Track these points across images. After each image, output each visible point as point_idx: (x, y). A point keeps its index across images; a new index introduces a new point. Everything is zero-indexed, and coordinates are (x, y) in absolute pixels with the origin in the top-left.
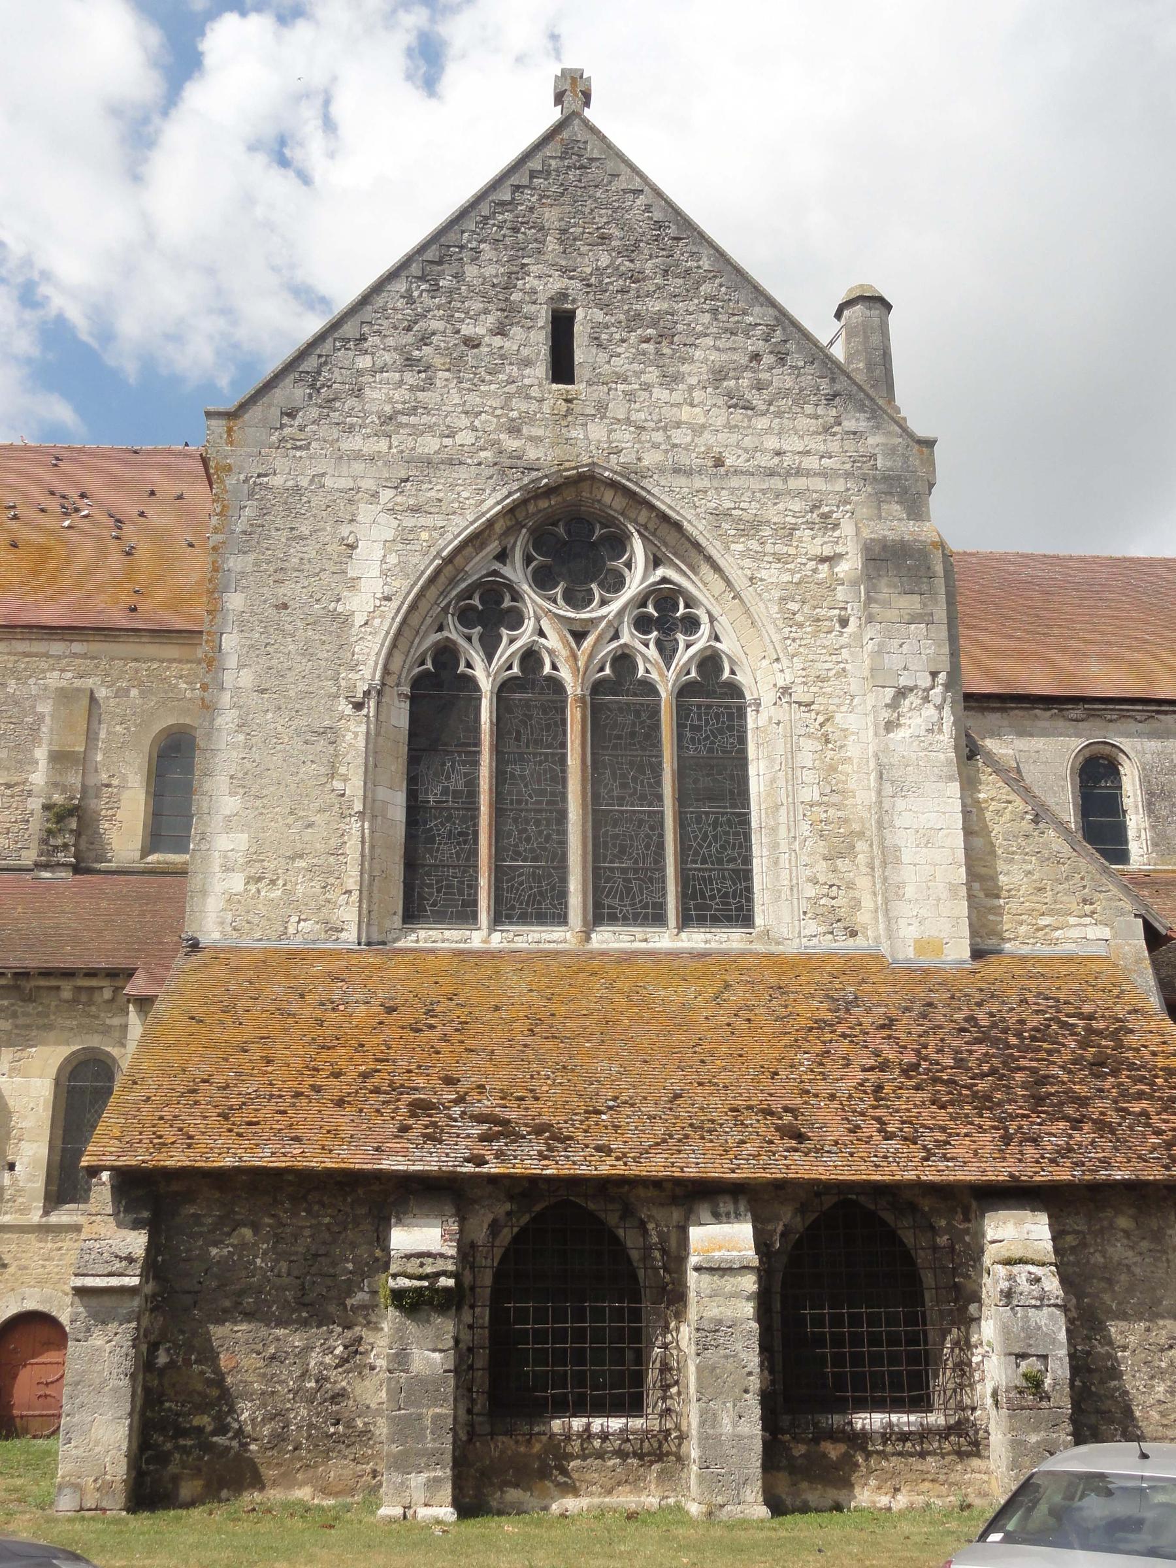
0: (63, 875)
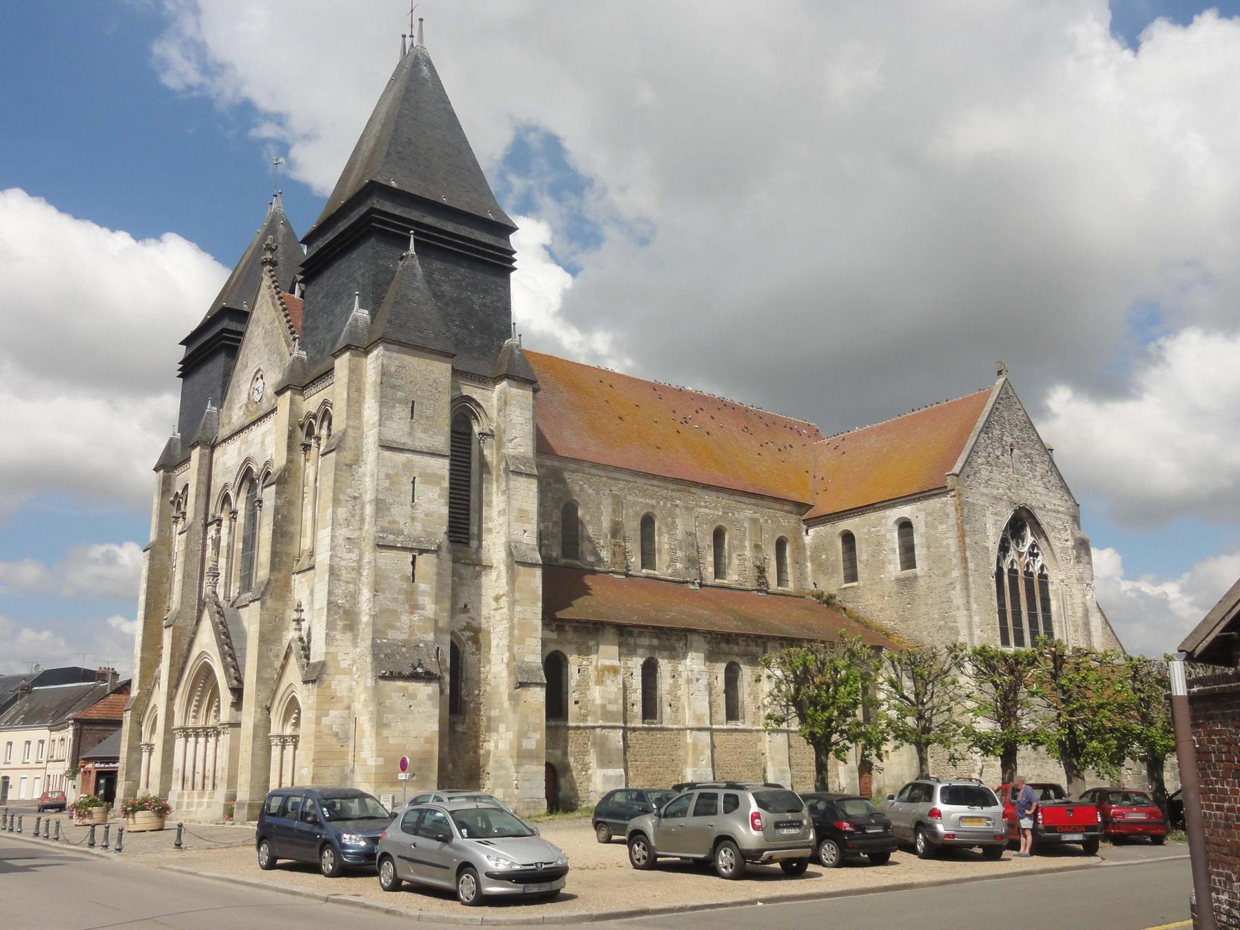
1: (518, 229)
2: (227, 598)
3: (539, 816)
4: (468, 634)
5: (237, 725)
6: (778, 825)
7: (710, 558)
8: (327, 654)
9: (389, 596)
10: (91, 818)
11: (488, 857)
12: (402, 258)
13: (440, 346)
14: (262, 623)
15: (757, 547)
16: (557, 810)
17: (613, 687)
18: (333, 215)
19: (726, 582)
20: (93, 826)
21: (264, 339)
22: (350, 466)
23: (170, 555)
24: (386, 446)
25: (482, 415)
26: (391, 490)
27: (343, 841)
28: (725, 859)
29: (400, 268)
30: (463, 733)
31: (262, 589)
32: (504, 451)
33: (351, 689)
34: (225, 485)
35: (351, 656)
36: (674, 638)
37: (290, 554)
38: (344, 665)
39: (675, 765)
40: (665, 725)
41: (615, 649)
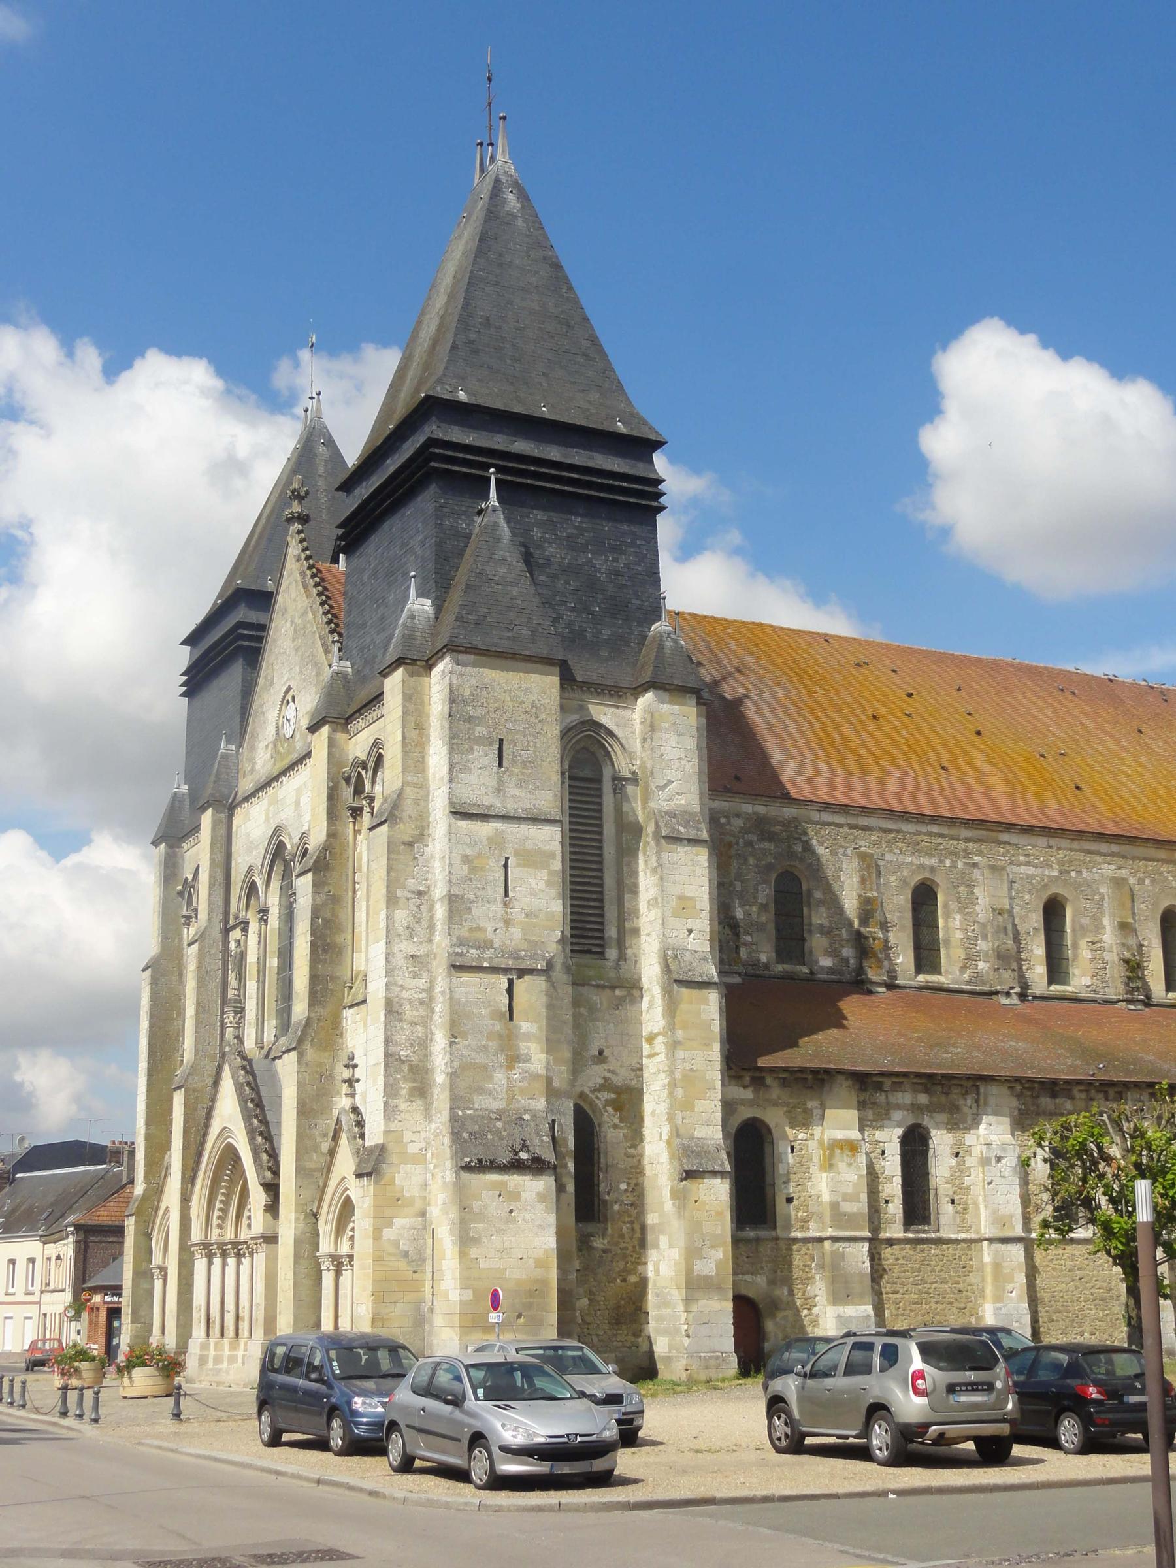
0: (1139, 1007)
1: (665, 443)
2: (260, 1045)
3: (723, 1380)
4: (606, 1096)
5: (271, 1239)
6: (951, 1389)
7: (1037, 950)
8: (387, 1133)
9: (474, 1044)
10: (80, 1378)
11: (503, 1425)
12: (480, 512)
13: (540, 649)
14: (300, 1084)
15: (1125, 927)
16: (758, 1371)
17: (852, 1174)
18: (379, 448)
19: (1068, 988)
20: (82, 1389)
21: (294, 639)
22: (411, 845)
23: (181, 975)
24: (461, 813)
25: (617, 748)
26: (470, 879)
27: (355, 1406)
28: (880, 1437)
29: (477, 530)
30: (605, 1251)
31: (299, 1033)
32: (652, 804)
33: (425, 1186)
34: (250, 869)
35: (423, 1135)
36: (955, 1091)
37: (338, 978)
38: (413, 1149)
39: (965, 1297)
40: (944, 1233)
41: (852, 1115)
